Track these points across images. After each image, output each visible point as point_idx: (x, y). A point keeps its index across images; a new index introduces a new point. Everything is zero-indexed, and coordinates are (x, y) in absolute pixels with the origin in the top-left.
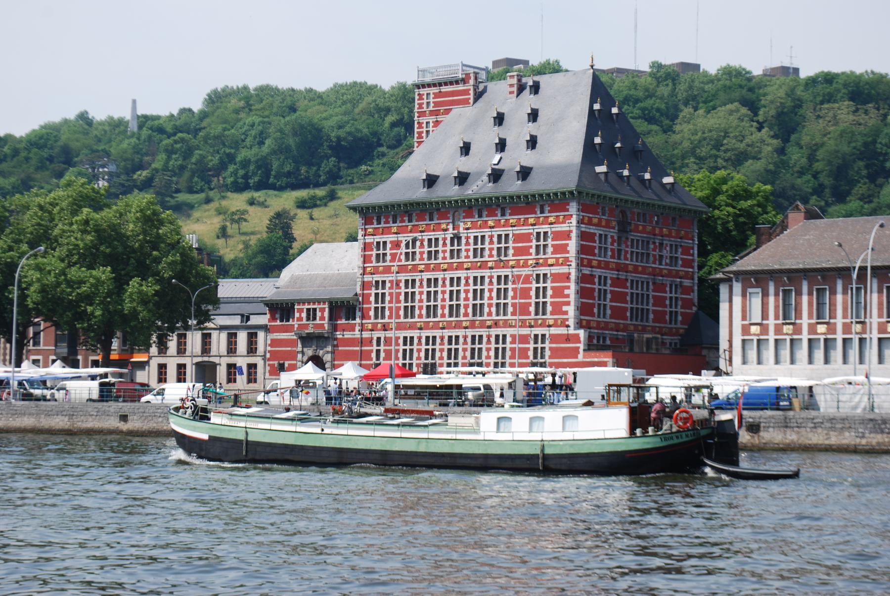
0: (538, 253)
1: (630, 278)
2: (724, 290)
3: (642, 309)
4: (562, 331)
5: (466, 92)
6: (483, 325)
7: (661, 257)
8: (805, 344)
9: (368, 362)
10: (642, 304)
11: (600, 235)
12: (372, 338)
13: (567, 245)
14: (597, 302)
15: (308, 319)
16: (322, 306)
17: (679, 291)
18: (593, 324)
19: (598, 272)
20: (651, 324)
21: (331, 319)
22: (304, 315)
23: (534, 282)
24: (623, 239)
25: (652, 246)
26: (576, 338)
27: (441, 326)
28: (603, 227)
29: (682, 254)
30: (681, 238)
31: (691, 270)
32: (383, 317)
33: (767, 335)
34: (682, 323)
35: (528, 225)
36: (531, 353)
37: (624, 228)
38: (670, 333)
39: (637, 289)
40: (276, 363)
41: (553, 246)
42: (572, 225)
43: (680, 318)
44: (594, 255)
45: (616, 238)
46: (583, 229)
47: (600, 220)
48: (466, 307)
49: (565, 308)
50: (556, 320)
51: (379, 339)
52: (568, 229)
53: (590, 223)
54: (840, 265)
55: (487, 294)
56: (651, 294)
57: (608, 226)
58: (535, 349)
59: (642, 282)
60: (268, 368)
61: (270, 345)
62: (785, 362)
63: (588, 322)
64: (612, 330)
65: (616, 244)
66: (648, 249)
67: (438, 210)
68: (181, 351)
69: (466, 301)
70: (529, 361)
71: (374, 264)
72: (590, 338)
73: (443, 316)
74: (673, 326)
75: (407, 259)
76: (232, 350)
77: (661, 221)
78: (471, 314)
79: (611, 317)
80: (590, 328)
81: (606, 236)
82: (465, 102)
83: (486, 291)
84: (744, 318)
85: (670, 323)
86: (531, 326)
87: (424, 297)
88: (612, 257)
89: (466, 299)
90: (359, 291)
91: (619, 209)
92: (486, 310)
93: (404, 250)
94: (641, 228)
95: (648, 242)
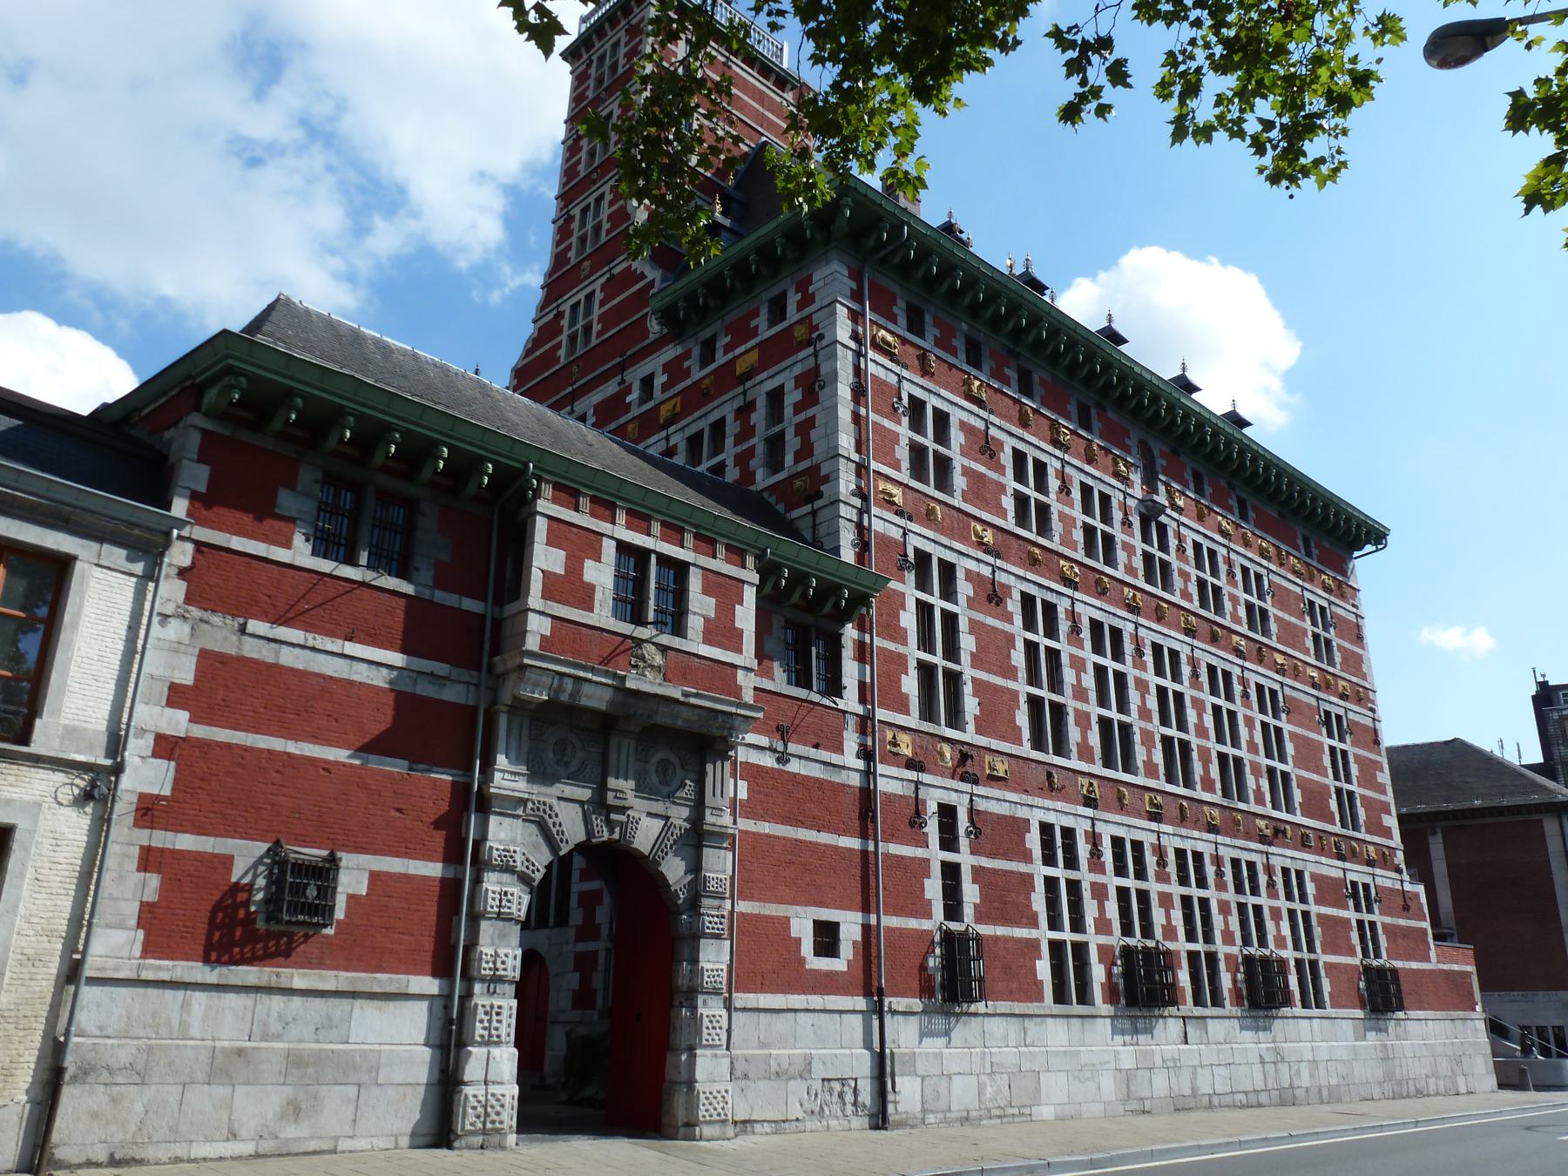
9: (913, 923)
16: (719, 565)
22: (601, 574)
60: (128, 887)
61: (176, 696)
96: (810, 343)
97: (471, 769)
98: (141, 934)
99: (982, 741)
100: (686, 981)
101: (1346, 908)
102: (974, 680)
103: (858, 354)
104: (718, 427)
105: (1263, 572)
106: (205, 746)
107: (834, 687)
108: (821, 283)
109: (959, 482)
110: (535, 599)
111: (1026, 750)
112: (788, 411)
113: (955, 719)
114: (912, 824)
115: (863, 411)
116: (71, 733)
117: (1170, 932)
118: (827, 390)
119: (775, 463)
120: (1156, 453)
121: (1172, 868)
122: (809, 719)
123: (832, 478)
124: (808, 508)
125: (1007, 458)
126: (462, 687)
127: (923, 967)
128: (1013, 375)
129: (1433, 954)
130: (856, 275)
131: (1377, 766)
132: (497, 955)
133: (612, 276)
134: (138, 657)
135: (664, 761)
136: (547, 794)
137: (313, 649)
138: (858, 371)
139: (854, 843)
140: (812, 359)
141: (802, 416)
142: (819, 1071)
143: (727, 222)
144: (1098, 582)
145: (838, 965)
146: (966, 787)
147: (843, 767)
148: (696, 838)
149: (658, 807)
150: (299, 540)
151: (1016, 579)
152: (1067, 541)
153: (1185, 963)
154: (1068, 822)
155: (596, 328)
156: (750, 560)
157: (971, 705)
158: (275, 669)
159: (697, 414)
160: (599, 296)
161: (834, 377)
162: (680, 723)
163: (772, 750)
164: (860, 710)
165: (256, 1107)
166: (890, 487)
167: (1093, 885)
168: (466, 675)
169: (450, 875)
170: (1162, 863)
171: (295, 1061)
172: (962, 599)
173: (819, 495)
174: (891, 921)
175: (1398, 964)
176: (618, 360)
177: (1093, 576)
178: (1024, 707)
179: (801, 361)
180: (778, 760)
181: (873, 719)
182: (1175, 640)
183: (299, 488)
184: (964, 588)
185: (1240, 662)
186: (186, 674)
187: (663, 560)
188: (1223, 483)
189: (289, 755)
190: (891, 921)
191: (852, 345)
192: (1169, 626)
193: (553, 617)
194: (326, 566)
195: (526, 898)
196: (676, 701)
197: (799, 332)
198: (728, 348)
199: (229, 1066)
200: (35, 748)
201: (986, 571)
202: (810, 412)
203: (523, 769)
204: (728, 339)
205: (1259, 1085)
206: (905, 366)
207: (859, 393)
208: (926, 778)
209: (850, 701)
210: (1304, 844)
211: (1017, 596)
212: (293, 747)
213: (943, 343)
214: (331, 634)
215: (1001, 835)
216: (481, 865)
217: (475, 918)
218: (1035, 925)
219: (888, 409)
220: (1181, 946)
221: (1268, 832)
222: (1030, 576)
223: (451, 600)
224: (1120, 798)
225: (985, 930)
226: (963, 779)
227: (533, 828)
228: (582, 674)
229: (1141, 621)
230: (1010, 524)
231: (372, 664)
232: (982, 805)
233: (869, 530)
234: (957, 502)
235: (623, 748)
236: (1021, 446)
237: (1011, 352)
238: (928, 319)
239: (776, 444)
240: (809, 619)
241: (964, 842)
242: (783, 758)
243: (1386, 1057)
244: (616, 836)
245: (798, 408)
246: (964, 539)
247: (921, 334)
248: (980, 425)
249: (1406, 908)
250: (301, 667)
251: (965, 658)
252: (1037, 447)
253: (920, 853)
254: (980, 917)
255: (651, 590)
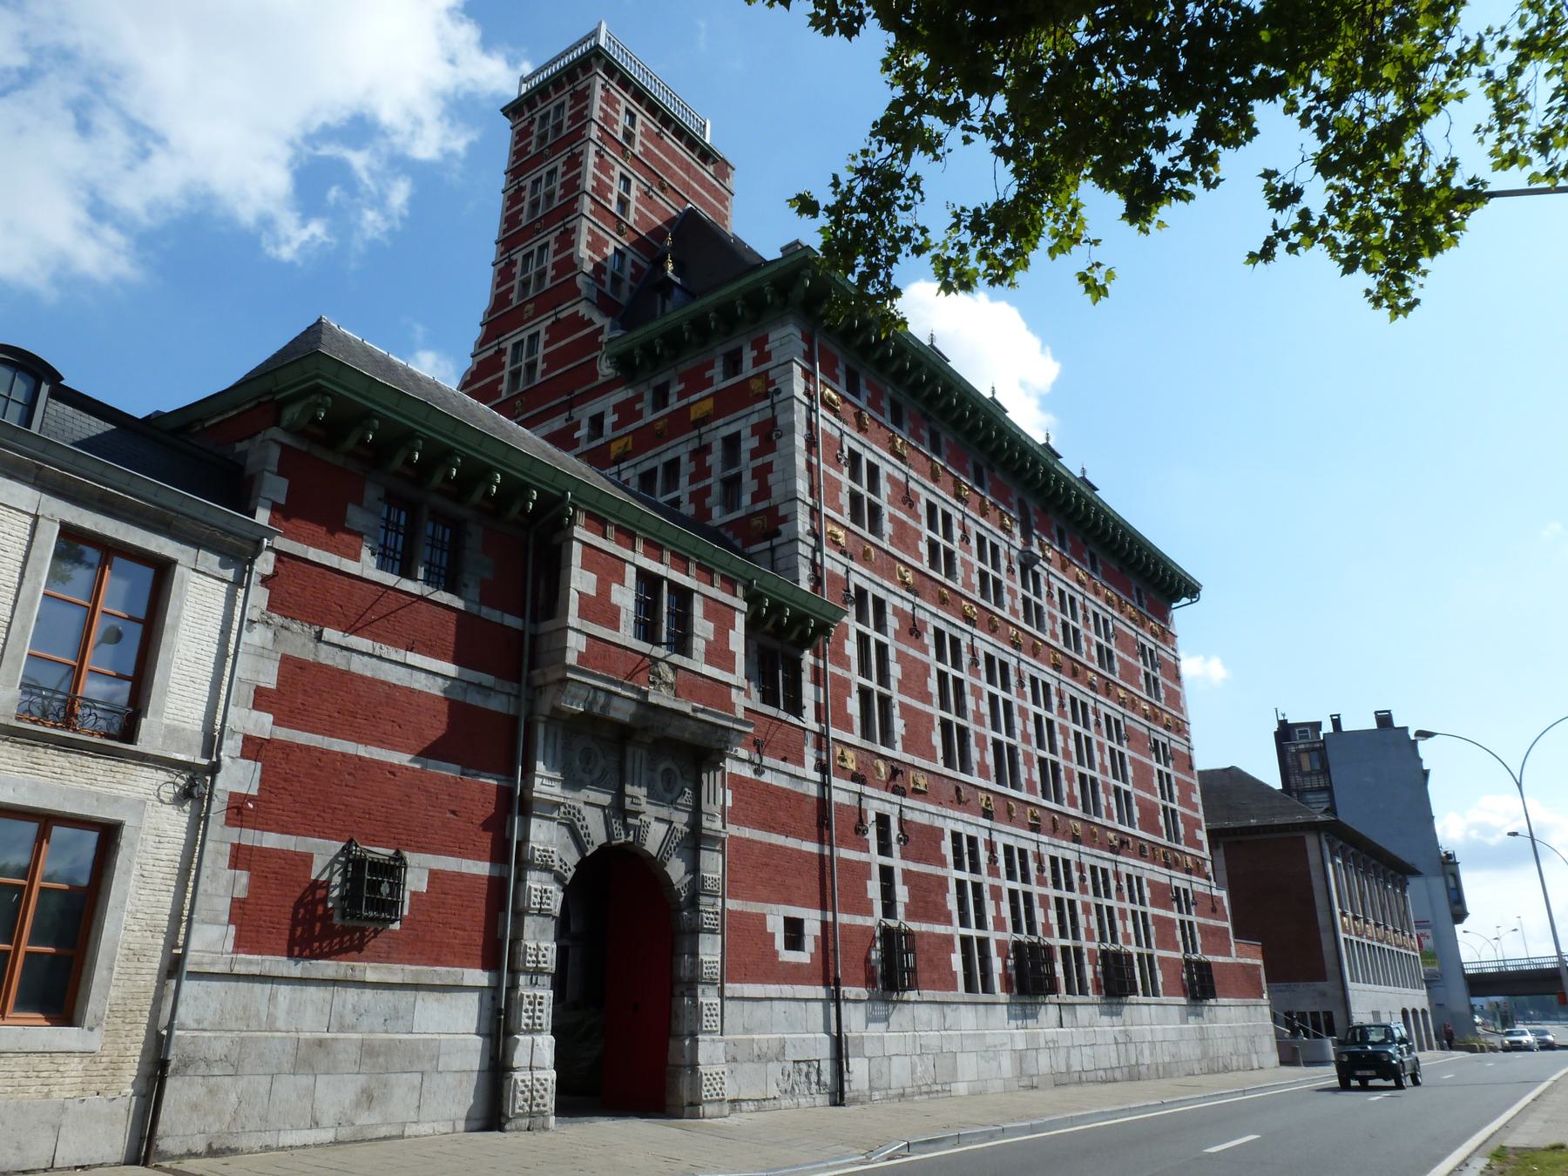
12: (861, 813)
16: (716, 593)
22: (625, 597)
60: (222, 885)
61: (262, 699)
96: (766, 396)
97: (514, 775)
98: (232, 929)
99: (908, 758)
100: (687, 973)
101: (1171, 909)
102: (901, 704)
103: (810, 409)
104: (672, 467)
105: (1109, 617)
106: (287, 748)
107: (796, 708)
108: (777, 344)
109: (887, 527)
110: (573, 619)
111: (939, 766)
112: (745, 456)
113: (887, 740)
114: (857, 831)
115: (814, 460)
116: (173, 733)
117: (1048, 929)
118: (783, 439)
119: (730, 503)
120: (1031, 510)
121: (1048, 874)
122: (779, 735)
123: (791, 518)
124: (767, 544)
125: (922, 509)
126: (504, 698)
127: (868, 960)
128: (926, 435)
129: (1233, 949)
130: (808, 339)
131: (1190, 787)
132: (539, 948)
133: (558, 320)
134: (230, 661)
135: (667, 770)
136: (576, 798)
137: (380, 658)
138: (810, 425)
139: (812, 847)
140: (769, 411)
141: (759, 462)
142: (791, 1055)
143: (678, 280)
144: (991, 621)
145: (803, 957)
146: (896, 798)
147: (805, 779)
148: (695, 841)
149: (664, 812)
150: (365, 553)
151: (932, 616)
152: (967, 584)
153: (1059, 957)
154: (972, 831)
155: (541, 366)
156: (740, 590)
157: (899, 726)
158: (346, 676)
159: (650, 453)
160: (543, 337)
161: (791, 428)
162: (687, 735)
163: (751, 762)
164: (816, 727)
165: (335, 1094)
166: (836, 529)
167: (992, 887)
168: (508, 686)
169: (496, 874)
170: (1041, 869)
171: (368, 1051)
172: (890, 632)
173: (778, 534)
174: (844, 918)
175: (1210, 958)
176: (565, 398)
177: (987, 616)
178: (938, 729)
179: (758, 412)
180: (756, 772)
181: (827, 736)
182: (1047, 675)
183: (365, 504)
184: (892, 622)
185: (1092, 694)
186: (270, 680)
187: (674, 586)
188: (1079, 540)
189: (360, 758)
190: (844, 918)
191: (805, 400)
192: (1042, 661)
193: (589, 635)
194: (390, 579)
195: (561, 895)
196: (685, 715)
197: (756, 386)
198: (681, 395)
199: (312, 1056)
200: (142, 746)
201: (908, 607)
202: (768, 458)
203: (557, 775)
204: (682, 386)
205: (1115, 1063)
206: (845, 422)
207: (811, 443)
208: (867, 790)
209: (809, 720)
210: (1141, 854)
211: (931, 631)
212: (363, 751)
213: (873, 403)
214: (394, 644)
215: (921, 841)
216: (524, 865)
217: (519, 915)
218: (949, 922)
219: (833, 459)
220: (1056, 941)
221: (1116, 843)
222: (941, 613)
223: (494, 615)
224: (1010, 811)
225: (915, 926)
226: (894, 792)
227: (564, 830)
228: (613, 688)
229: (1023, 656)
230: (924, 566)
231: (427, 674)
232: (909, 815)
233: (822, 567)
234: (886, 545)
235: (636, 757)
236: (933, 499)
237: (925, 416)
238: (862, 382)
239: (732, 485)
240: (777, 645)
241: (896, 848)
242: (759, 770)
243: (1203, 1038)
244: (631, 839)
245: (755, 454)
246: (891, 578)
247: (857, 395)
248: (902, 478)
249: (1214, 910)
250: (369, 674)
251: (894, 684)
252: (945, 501)
253: (863, 857)
254: (911, 915)
255: (664, 613)
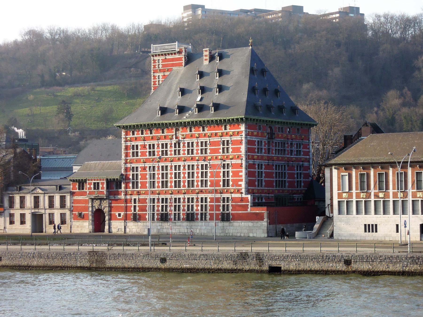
0: (223, 152)
1: (275, 164)
2: (327, 171)
3: (282, 181)
4: (238, 195)
5: (180, 59)
6: (193, 192)
7: (292, 151)
8: (373, 204)
10: (282, 178)
11: (258, 141)
12: (131, 199)
13: (240, 148)
14: (257, 178)
15: (95, 189)
17: (302, 169)
18: (255, 191)
19: (257, 162)
20: (287, 189)
21: (107, 188)
22: (92, 186)
23: (222, 168)
24: (271, 142)
25: (286, 145)
26: (246, 200)
27: (170, 192)
28: (260, 136)
29: (303, 148)
30: (302, 140)
31: (308, 157)
32: (137, 187)
33: (352, 199)
34: (304, 187)
35: (218, 137)
36: (221, 208)
37: (271, 136)
38: (297, 193)
39: (279, 170)
40: (77, 213)
41: (232, 148)
42: (243, 137)
43: (302, 184)
44: (255, 152)
45: (267, 142)
46: (249, 139)
47: (258, 133)
48: (184, 182)
49: (240, 183)
50: (235, 189)
51: (135, 200)
52: (240, 139)
53: (252, 135)
54: (390, 161)
55: (196, 175)
56: (287, 172)
57: (262, 136)
58: (224, 206)
59: (282, 166)
62: (362, 213)
63: (253, 190)
64: (266, 193)
65: (267, 146)
66: (284, 146)
67: (167, 127)
68: (22, 206)
69: (184, 179)
70: (220, 212)
71: (131, 158)
72: (254, 199)
73: (171, 186)
74: (299, 189)
75: (150, 155)
76: (51, 205)
77: (291, 131)
78: (187, 186)
79: (265, 186)
80: (253, 193)
81: (261, 141)
82: (180, 65)
83: (195, 173)
84: (339, 189)
85: (297, 187)
86: (221, 193)
87: (160, 176)
88: (265, 153)
89: (184, 177)
90: (123, 172)
91: (268, 126)
92: (195, 184)
93: (148, 150)
94: (280, 135)
95: (284, 143)
99: (141, 189)
139: (128, 205)
145: (121, 217)
242: (115, 197)
